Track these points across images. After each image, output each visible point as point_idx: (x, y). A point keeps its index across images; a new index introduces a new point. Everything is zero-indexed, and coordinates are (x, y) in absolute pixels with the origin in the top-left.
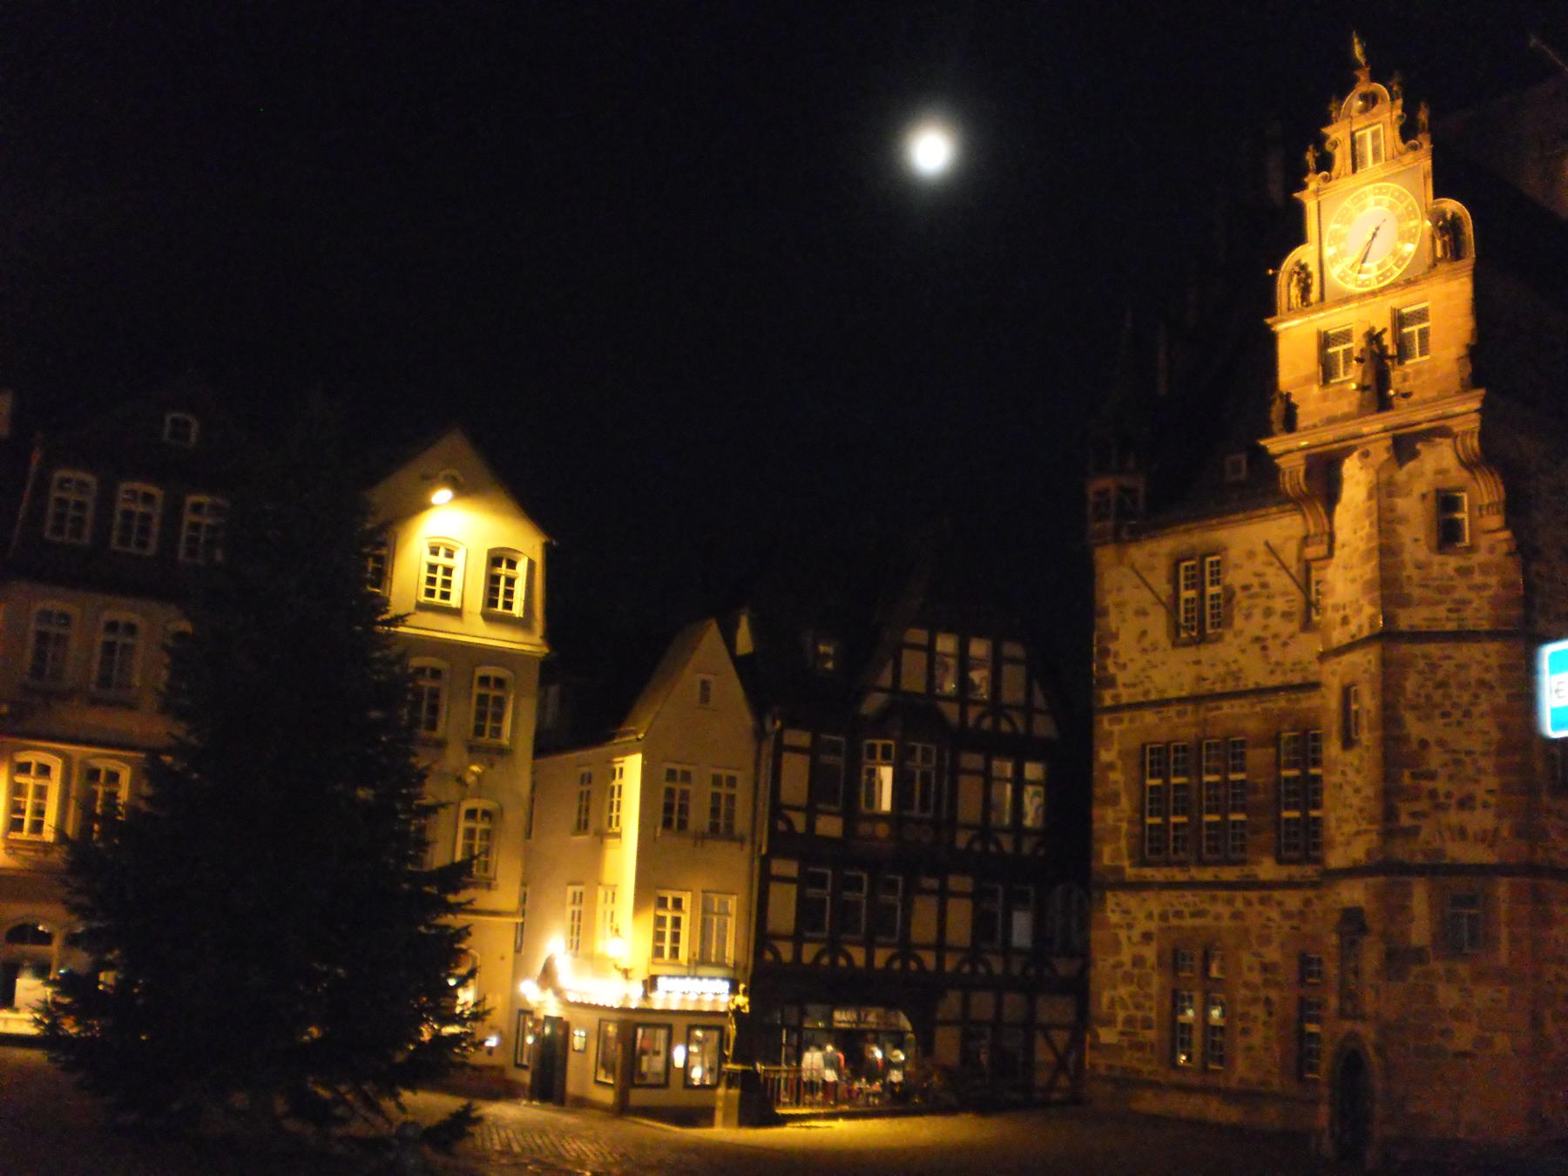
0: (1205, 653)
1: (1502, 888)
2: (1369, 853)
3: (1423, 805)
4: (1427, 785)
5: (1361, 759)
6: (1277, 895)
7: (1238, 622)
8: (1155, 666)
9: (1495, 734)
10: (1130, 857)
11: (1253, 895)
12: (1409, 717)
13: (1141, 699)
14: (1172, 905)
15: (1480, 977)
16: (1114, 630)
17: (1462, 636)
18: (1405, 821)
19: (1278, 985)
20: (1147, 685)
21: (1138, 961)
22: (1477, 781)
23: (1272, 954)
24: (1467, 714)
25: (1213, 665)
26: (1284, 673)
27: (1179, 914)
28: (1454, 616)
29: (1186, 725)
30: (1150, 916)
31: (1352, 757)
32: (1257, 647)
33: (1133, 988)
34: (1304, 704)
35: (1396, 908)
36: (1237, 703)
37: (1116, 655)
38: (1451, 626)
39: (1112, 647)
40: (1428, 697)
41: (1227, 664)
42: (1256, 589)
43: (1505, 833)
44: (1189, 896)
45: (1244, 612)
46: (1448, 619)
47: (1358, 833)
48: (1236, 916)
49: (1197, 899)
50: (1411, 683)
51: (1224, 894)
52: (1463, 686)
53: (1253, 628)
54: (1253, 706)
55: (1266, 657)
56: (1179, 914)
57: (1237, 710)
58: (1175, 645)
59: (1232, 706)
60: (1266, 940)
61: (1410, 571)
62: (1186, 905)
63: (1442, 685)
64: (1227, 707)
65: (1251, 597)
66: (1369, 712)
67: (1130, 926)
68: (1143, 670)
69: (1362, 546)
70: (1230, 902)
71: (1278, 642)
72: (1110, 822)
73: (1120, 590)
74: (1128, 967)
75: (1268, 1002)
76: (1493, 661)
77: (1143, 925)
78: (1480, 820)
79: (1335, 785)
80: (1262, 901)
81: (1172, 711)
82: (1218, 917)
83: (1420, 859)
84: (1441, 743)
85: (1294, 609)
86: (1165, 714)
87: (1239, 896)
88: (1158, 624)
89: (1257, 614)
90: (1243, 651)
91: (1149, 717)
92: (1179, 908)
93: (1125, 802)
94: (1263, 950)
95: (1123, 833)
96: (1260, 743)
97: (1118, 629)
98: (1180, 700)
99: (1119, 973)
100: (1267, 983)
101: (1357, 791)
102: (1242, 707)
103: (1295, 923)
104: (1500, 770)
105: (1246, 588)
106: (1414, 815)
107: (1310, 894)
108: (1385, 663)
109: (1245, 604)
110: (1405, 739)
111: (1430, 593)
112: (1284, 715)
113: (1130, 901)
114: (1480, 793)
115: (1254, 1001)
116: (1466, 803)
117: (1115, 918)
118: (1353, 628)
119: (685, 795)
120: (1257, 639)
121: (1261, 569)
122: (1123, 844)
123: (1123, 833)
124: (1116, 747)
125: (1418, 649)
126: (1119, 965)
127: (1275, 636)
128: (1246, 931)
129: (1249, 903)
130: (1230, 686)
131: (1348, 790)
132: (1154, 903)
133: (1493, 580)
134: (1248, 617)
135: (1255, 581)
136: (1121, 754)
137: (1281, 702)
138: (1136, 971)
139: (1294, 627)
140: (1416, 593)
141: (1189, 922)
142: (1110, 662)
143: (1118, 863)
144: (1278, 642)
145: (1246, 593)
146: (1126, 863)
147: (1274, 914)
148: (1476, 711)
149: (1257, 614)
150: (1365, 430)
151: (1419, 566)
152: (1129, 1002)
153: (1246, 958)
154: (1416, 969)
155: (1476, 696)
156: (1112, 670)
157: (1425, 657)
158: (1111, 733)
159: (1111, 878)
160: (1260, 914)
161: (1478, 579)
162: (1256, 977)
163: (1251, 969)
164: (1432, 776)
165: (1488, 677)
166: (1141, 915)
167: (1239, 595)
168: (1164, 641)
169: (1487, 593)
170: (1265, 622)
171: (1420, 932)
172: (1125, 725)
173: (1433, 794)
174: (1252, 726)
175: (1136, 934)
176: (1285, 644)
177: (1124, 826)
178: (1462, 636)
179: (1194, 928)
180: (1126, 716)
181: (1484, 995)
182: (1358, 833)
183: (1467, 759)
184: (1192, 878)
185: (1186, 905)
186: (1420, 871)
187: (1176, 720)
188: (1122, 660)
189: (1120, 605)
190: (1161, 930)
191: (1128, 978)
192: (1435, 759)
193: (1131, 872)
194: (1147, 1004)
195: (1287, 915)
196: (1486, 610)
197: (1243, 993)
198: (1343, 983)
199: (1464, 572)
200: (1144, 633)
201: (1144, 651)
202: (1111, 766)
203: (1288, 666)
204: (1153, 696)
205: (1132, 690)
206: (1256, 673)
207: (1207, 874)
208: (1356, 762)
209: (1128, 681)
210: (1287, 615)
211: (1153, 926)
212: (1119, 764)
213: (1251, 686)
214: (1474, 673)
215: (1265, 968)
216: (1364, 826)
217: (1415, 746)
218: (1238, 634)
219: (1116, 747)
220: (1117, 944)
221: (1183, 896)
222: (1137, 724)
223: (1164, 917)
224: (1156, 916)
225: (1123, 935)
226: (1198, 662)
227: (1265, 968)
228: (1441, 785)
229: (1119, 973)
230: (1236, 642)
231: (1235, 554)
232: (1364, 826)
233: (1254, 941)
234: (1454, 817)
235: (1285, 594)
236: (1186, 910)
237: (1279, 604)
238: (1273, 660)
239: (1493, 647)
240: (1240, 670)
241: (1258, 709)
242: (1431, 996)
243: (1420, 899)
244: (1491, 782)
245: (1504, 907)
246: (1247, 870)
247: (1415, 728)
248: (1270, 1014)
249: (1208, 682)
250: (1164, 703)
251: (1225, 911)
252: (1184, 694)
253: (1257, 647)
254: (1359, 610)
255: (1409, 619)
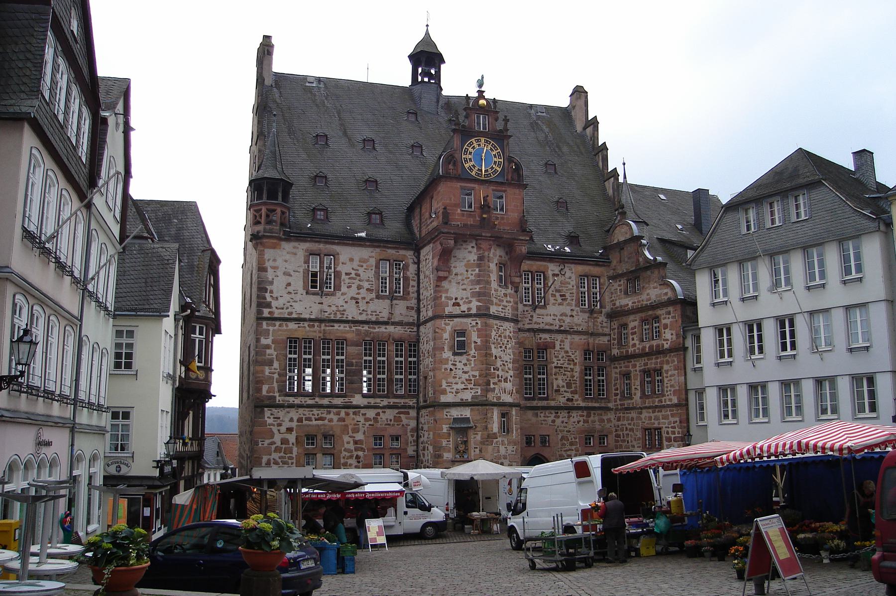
0: (326, 300)
1: (514, 411)
2: (473, 397)
3: (496, 380)
4: (497, 372)
5: (468, 360)
6: (363, 411)
7: (344, 289)
8: (297, 302)
9: (512, 356)
10: (279, 391)
11: (351, 411)
12: (493, 346)
13: (286, 316)
14: (304, 415)
15: (509, 443)
16: (270, 279)
17: (505, 319)
18: (492, 386)
19: (362, 450)
20: (290, 310)
21: (284, 441)
22: (508, 372)
23: (359, 436)
24: (506, 347)
25: (330, 306)
26: (367, 315)
27: (309, 419)
28: (503, 311)
29: (315, 332)
30: (291, 420)
31: (464, 359)
32: (354, 301)
33: (282, 454)
34: (377, 330)
35: (486, 419)
36: (342, 325)
37: (271, 292)
38: (502, 315)
39: (269, 288)
40: (497, 340)
41: (337, 306)
42: (353, 275)
43: (514, 391)
44: (315, 411)
45: (347, 285)
46: (502, 312)
47: (467, 389)
48: (343, 420)
49: (319, 412)
50: (493, 333)
51: (335, 410)
52: (505, 337)
53: (353, 292)
54: (350, 327)
55: (358, 306)
56: (309, 419)
57: (342, 328)
58: (307, 293)
59: (340, 326)
60: (356, 430)
61: (493, 292)
62: (313, 414)
63: (500, 336)
64: (336, 326)
65: (350, 278)
66: (475, 342)
67: (280, 425)
68: (289, 302)
69: (472, 278)
70: (338, 414)
71: (365, 301)
72: (267, 373)
73: (275, 260)
74: (279, 444)
75: (358, 457)
76: (512, 329)
77: (287, 424)
78: (509, 386)
79: (446, 369)
80: (354, 413)
81: (306, 324)
82: (331, 420)
83: (495, 400)
84: (500, 358)
85: (374, 288)
86: (301, 325)
87: (343, 412)
88: (298, 283)
89: (354, 287)
90: (346, 302)
91: (292, 326)
92: (308, 416)
93: (276, 365)
94: (354, 435)
95: (275, 380)
96: (358, 344)
97: (273, 279)
98: (311, 320)
99: (273, 447)
100: (356, 449)
101: (466, 373)
102: (345, 327)
103: (371, 423)
104: (514, 369)
105: (346, 274)
106: (493, 383)
107: (380, 411)
108: (486, 325)
109: (347, 281)
110: (491, 355)
111: (497, 301)
112: (367, 333)
113: (281, 413)
114: (509, 377)
115: (351, 457)
116: (506, 380)
117: (270, 421)
118: (464, 308)
119: (130, 346)
120: (352, 298)
121: (356, 267)
122: (275, 385)
123: (275, 380)
124: (271, 338)
125: (497, 322)
126: (273, 443)
127: (364, 298)
128: (347, 426)
129: (347, 414)
130: (339, 317)
131: (460, 372)
132: (294, 414)
133: (512, 300)
134: (349, 287)
135: (353, 272)
136: (273, 342)
137: (366, 327)
138: (284, 446)
139: (373, 295)
140: (495, 300)
141: (314, 422)
142: (268, 295)
143: (271, 394)
144: (365, 301)
145: (348, 277)
146: (277, 394)
147: (361, 419)
148: (508, 347)
149: (354, 287)
150: (483, 234)
151: (496, 290)
152: (279, 461)
153: (346, 438)
154: (495, 440)
155: (508, 341)
156: (269, 299)
157: (496, 325)
158: (269, 330)
159: (267, 402)
160: (353, 419)
161: (508, 299)
162: (351, 446)
163: (348, 443)
164: (498, 370)
165: (511, 335)
166: (287, 420)
167: (343, 276)
168: (301, 290)
169: (510, 304)
170: (357, 291)
171: (495, 427)
172: (275, 328)
173: (498, 376)
174: (349, 336)
175: (283, 429)
176: (367, 303)
177: (276, 376)
178: (505, 319)
179: (318, 425)
180: (278, 323)
181: (510, 448)
182: (464, 389)
183: (506, 364)
184: (317, 402)
185: (313, 414)
186: (494, 405)
187: (308, 328)
188: (275, 295)
189: (275, 268)
190: (296, 426)
191: (278, 450)
192: (499, 363)
193: (279, 399)
194: (290, 461)
195: (367, 420)
196: (510, 311)
197: (344, 453)
198: (456, 448)
199: (505, 295)
200: (289, 284)
201: (289, 293)
202: (268, 347)
203: (369, 312)
204: (294, 316)
205: (281, 311)
206: (352, 312)
207: (326, 401)
208: (464, 361)
209: (279, 307)
210: (367, 290)
211: (294, 424)
212: (273, 346)
213: (350, 318)
214: (507, 333)
215: (356, 442)
216: (472, 386)
217: (494, 358)
218: (342, 294)
219: (271, 338)
220: (272, 435)
221: (312, 411)
222: (285, 328)
223: (300, 420)
224: (295, 419)
225: (275, 429)
226: (322, 303)
227: (356, 442)
228: (500, 373)
229: (273, 447)
230: (342, 298)
231: (343, 258)
232: (469, 386)
233: (350, 430)
234: (503, 384)
235: (368, 281)
236: (313, 417)
237: (366, 285)
238: (361, 309)
239: (512, 324)
240: (344, 310)
241: (354, 328)
242: (499, 452)
243: (496, 414)
244: (511, 373)
245: (514, 418)
246: (347, 400)
247: (494, 351)
248: (359, 462)
249: (328, 313)
250: (299, 320)
251: (335, 418)
252: (313, 317)
253: (354, 301)
254: (470, 302)
255: (493, 310)
